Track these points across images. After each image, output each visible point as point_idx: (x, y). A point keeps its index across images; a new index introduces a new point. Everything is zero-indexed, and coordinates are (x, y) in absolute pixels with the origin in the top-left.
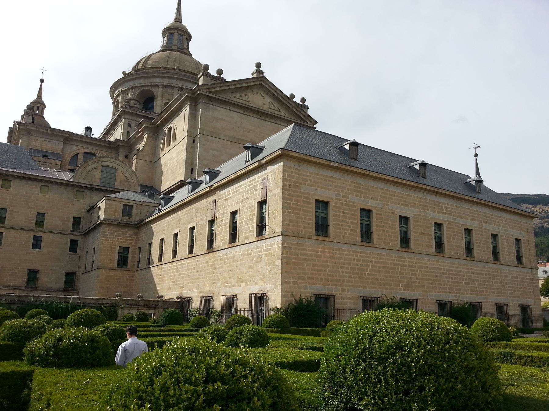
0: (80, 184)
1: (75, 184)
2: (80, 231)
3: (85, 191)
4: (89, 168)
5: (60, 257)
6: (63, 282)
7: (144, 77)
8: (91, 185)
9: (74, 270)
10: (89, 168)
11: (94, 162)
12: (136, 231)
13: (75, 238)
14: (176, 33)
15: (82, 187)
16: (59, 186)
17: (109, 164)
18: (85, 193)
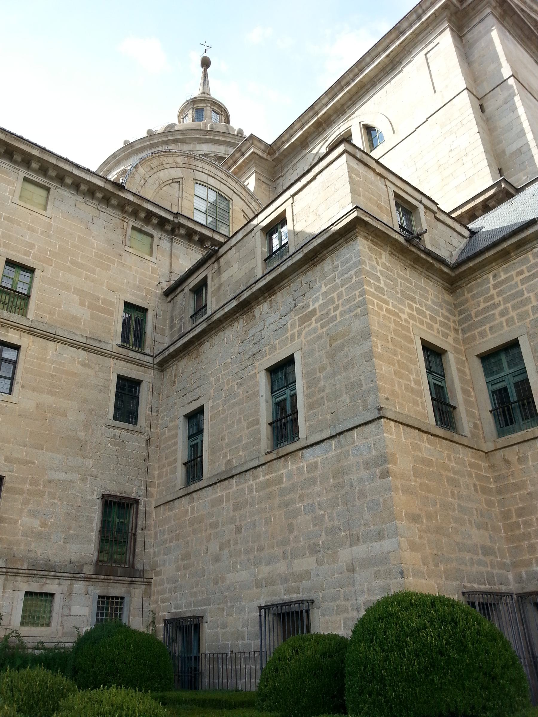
0: (146, 205)
1: (131, 198)
2: (147, 351)
3: (157, 234)
4: (164, 175)
5: (82, 435)
6: (94, 535)
7: (175, 141)
8: (177, 215)
9: (133, 490)
10: (164, 175)
11: (177, 165)
12: (447, 297)
13: (132, 372)
14: (209, 108)
15: (150, 215)
16: (80, 198)
17: (211, 181)
18: (156, 240)
